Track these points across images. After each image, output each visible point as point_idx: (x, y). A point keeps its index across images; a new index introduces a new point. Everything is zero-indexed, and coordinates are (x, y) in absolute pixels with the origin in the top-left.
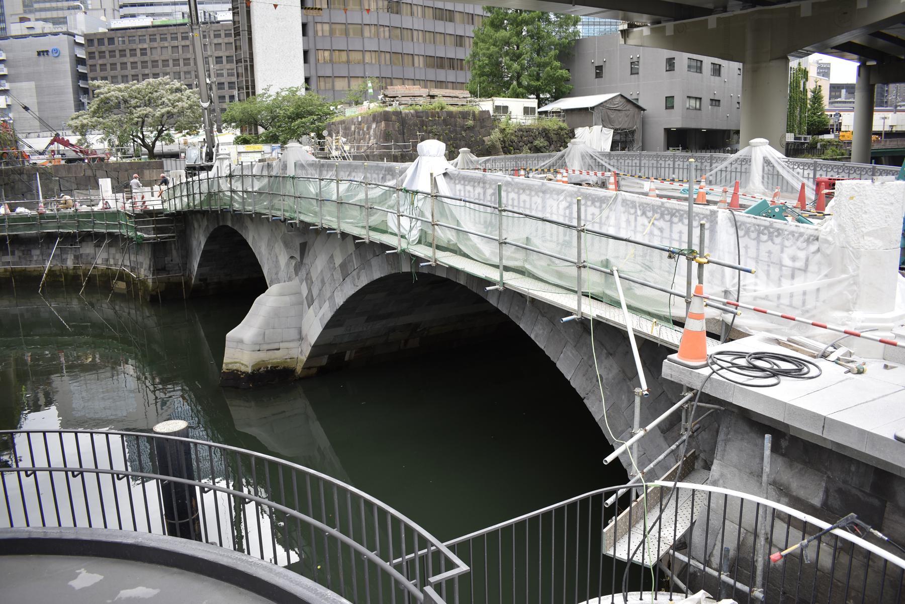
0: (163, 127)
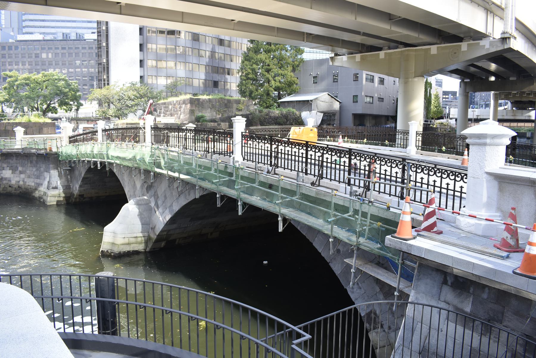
0: (51, 102)
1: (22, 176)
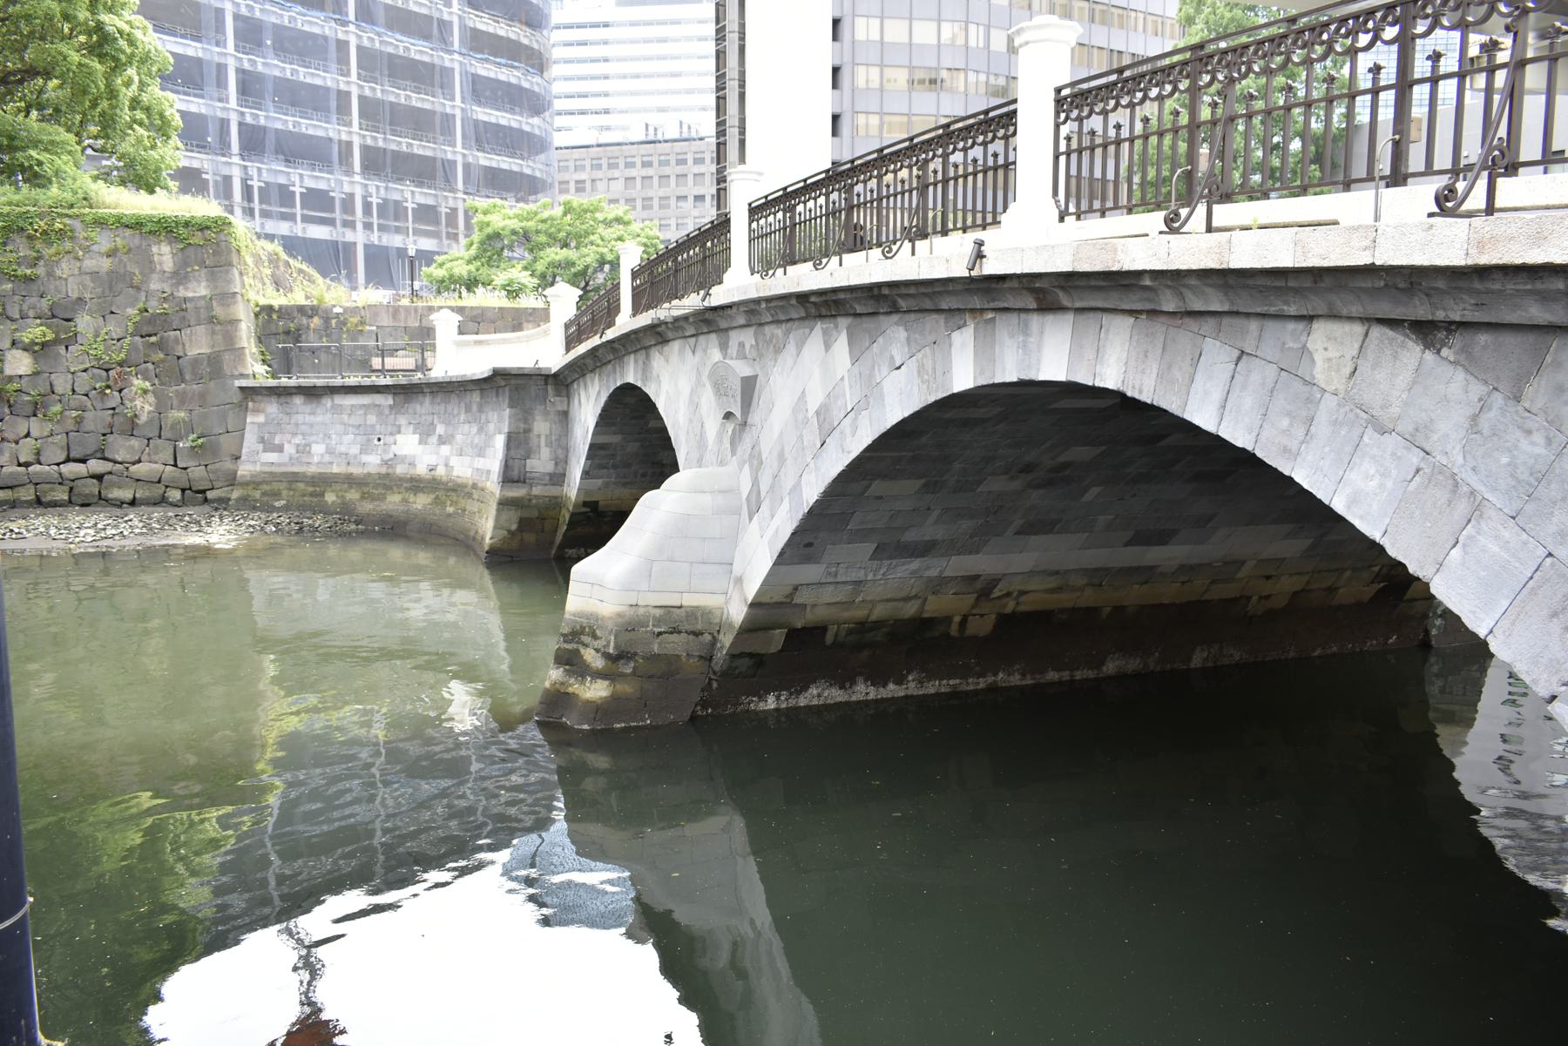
1: (445, 450)
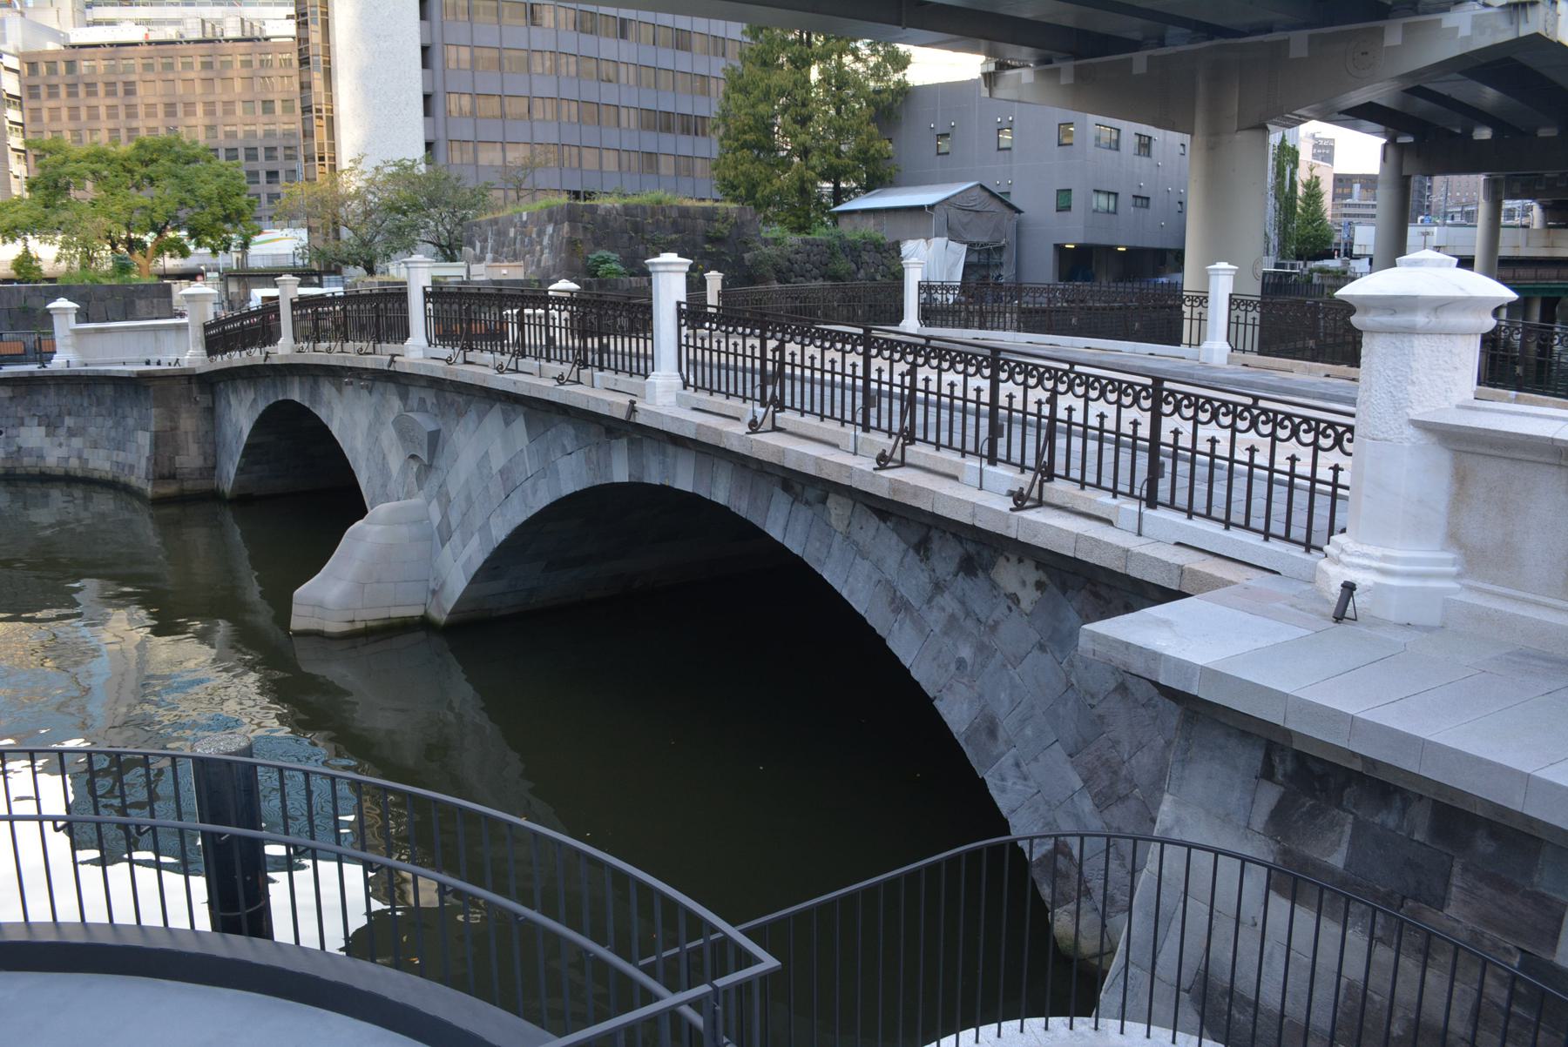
1: (77, 442)
